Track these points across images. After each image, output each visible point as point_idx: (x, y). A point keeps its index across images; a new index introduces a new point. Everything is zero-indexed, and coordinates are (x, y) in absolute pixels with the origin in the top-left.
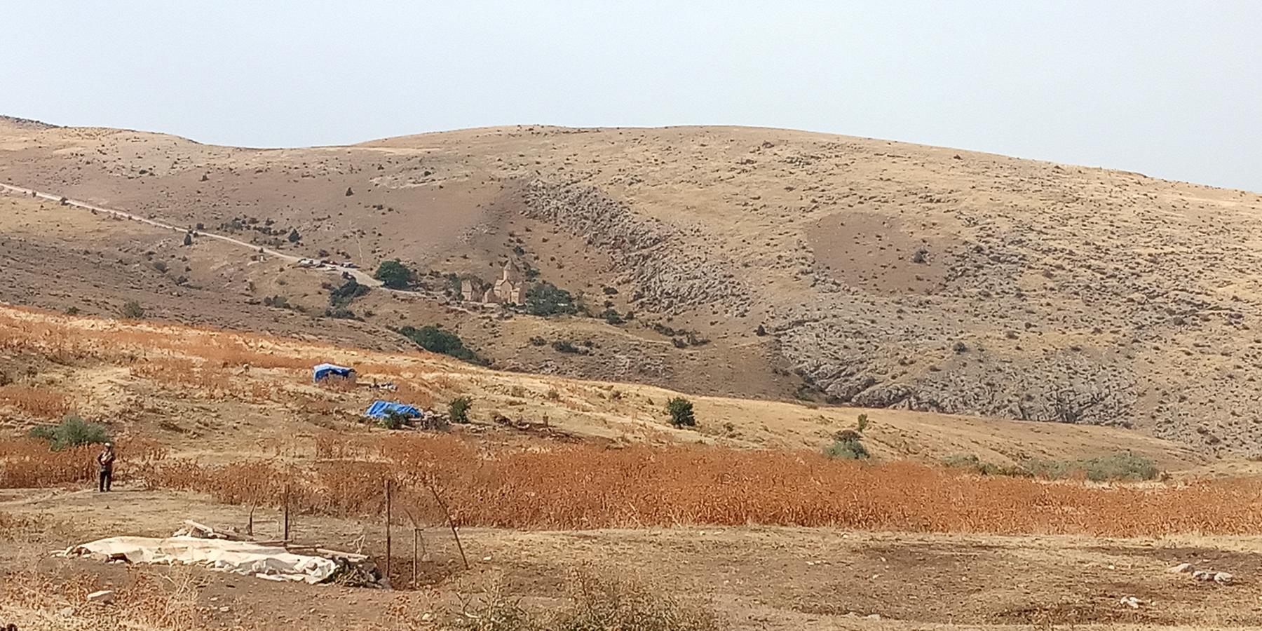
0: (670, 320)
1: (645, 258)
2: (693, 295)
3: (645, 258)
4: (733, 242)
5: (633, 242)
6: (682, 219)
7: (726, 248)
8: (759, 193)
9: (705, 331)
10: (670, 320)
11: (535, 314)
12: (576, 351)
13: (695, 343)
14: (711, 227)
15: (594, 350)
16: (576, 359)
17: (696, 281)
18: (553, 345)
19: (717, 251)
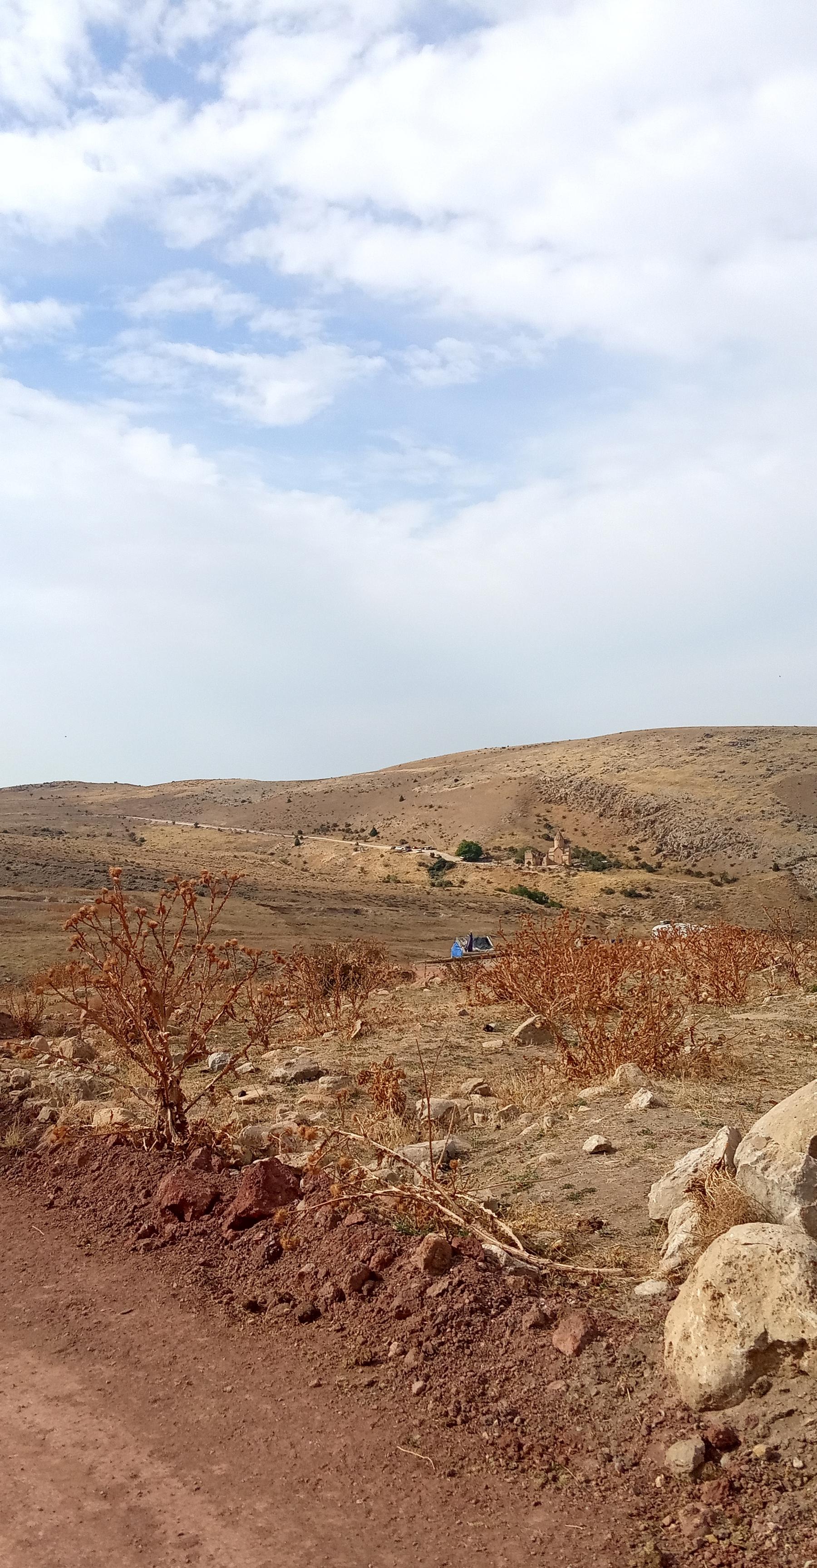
0: (694, 865)
1: (653, 822)
2: (705, 844)
3: (653, 822)
4: (721, 804)
5: (638, 812)
6: (670, 793)
7: (718, 809)
8: (722, 768)
9: (731, 873)
10: (694, 865)
11: (594, 870)
12: (640, 896)
13: (729, 882)
14: (698, 795)
15: (654, 894)
16: (642, 901)
17: (703, 835)
18: (621, 893)
19: (711, 812)
